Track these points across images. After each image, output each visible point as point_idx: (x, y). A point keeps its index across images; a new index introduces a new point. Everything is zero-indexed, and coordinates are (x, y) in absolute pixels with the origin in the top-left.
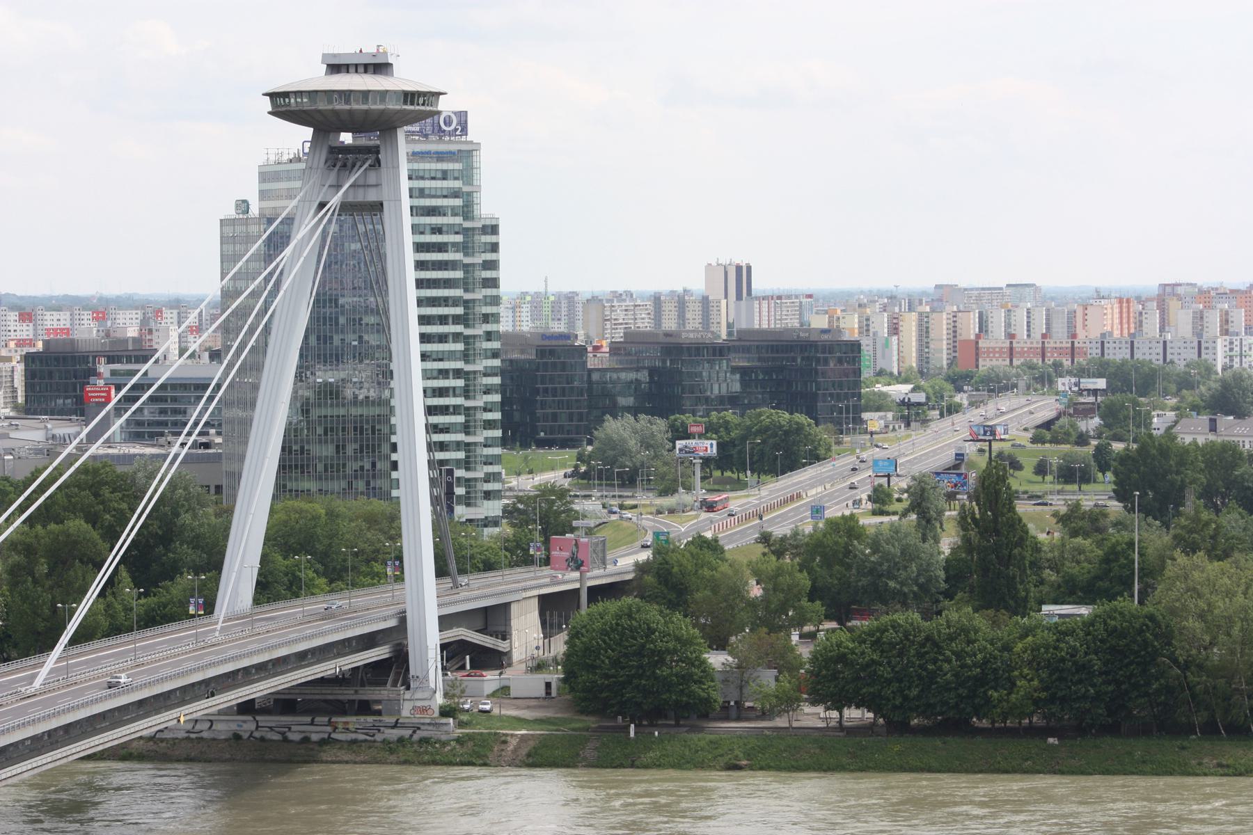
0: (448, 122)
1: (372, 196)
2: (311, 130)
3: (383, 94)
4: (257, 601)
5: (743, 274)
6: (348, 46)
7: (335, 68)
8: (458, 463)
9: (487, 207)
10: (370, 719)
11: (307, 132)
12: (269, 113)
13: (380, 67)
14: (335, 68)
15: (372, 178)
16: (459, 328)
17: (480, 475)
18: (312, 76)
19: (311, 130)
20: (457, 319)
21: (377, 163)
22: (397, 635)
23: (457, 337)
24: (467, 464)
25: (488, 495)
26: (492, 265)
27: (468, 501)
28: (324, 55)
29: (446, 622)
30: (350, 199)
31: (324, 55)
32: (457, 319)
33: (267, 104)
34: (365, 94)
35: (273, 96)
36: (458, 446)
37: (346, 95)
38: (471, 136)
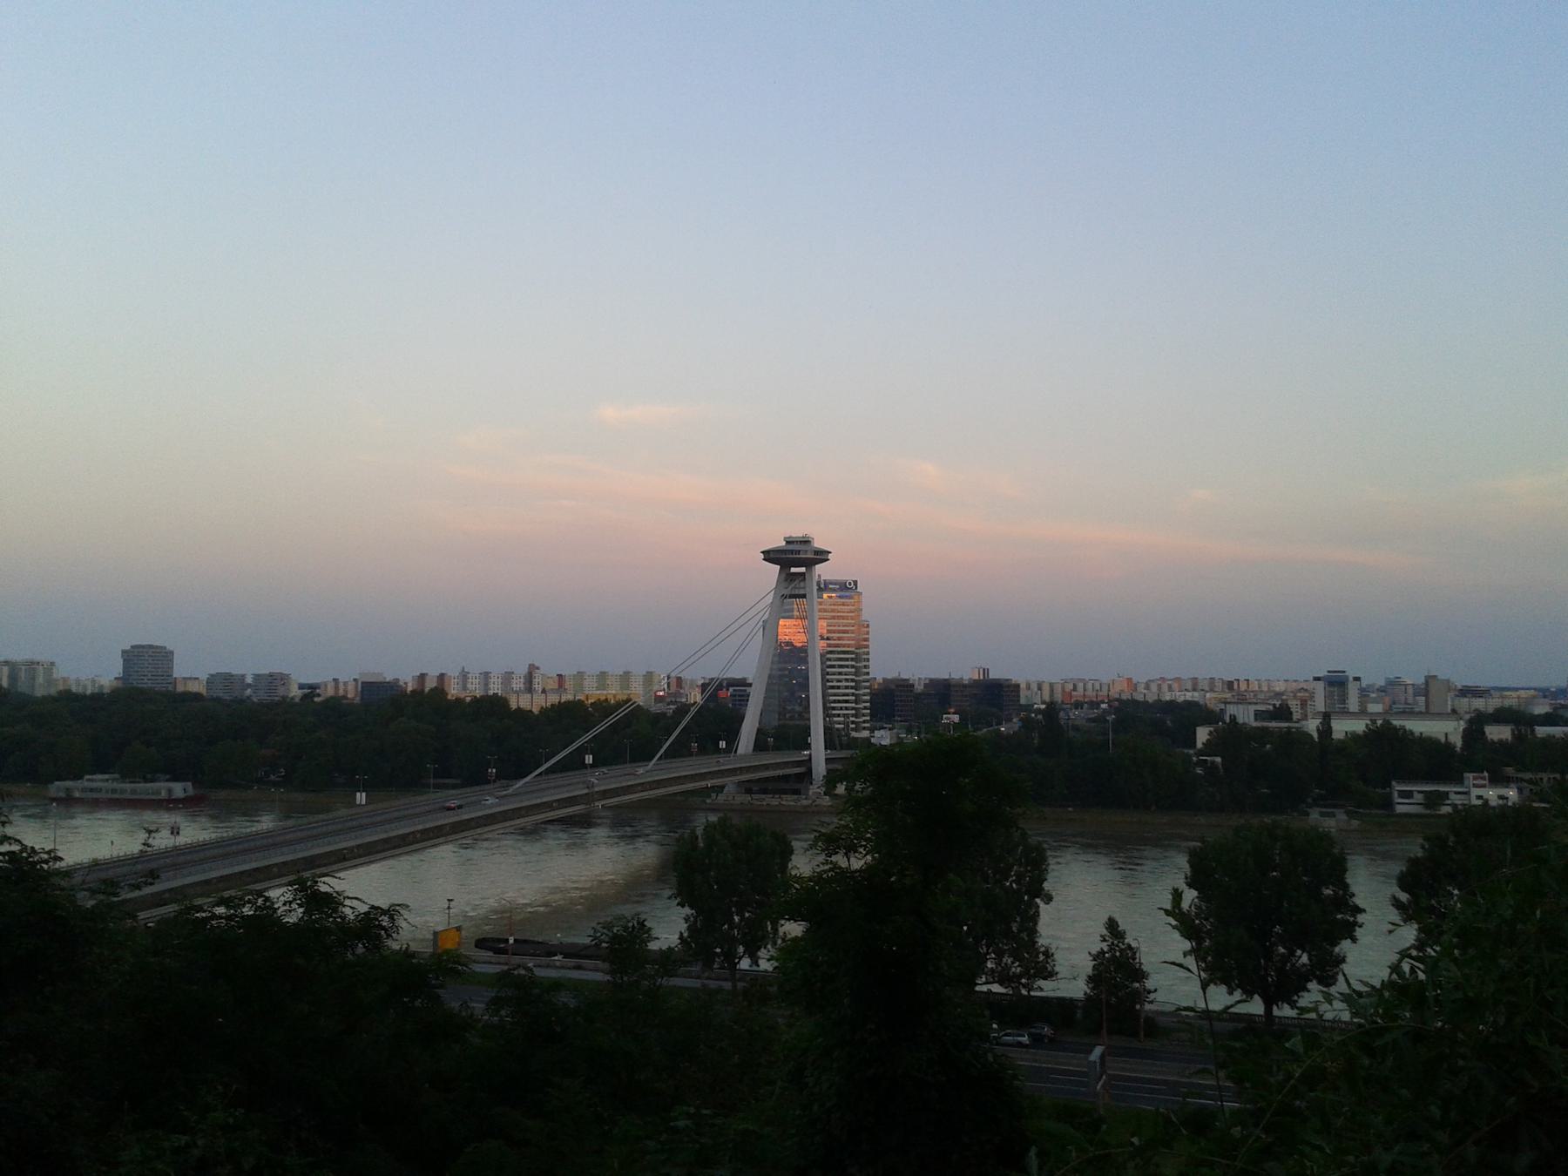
0: (850, 584)
1: (802, 592)
2: (779, 567)
4: (754, 750)
5: (986, 671)
6: (797, 533)
8: (853, 715)
9: (865, 616)
10: (796, 797)
12: (764, 559)
16: (853, 663)
17: (861, 720)
19: (779, 567)
20: (852, 659)
21: (805, 579)
23: (853, 666)
24: (856, 716)
26: (866, 640)
27: (856, 730)
28: (785, 538)
30: (793, 593)
31: (785, 538)
32: (852, 659)
33: (762, 556)
36: (853, 708)
37: (792, 552)
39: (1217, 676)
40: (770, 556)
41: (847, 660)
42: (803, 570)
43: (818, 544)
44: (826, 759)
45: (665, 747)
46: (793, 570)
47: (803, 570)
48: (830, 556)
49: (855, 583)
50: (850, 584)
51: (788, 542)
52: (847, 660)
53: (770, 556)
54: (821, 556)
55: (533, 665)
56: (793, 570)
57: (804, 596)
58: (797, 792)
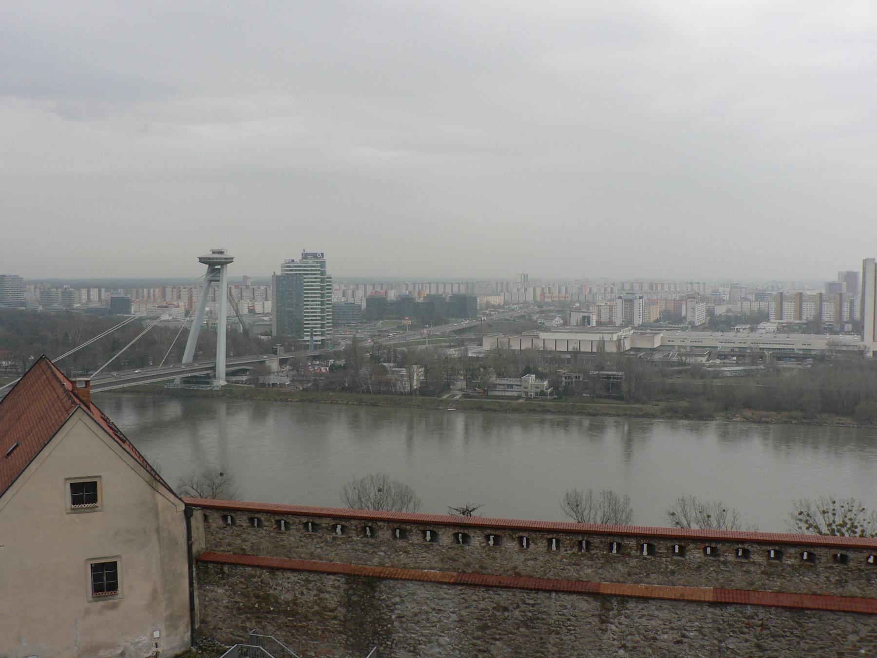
0: (319, 255)
1: (218, 279)
3: (221, 258)
6: (218, 248)
11: (208, 265)
13: (221, 253)
14: (214, 253)
15: (218, 275)
18: (207, 254)
21: (219, 272)
22: (213, 368)
25: (328, 334)
29: (227, 366)
31: (211, 250)
32: (319, 297)
34: (217, 258)
35: (200, 259)
37: (213, 258)
38: (324, 258)
40: (202, 260)
41: (316, 297)
43: (228, 254)
44: (226, 365)
46: (217, 267)
48: (234, 260)
49: (322, 254)
50: (319, 255)
51: (214, 253)
52: (316, 297)
53: (202, 260)
54: (229, 260)
55: (246, 276)
56: (217, 267)
57: (219, 281)
58: (208, 383)
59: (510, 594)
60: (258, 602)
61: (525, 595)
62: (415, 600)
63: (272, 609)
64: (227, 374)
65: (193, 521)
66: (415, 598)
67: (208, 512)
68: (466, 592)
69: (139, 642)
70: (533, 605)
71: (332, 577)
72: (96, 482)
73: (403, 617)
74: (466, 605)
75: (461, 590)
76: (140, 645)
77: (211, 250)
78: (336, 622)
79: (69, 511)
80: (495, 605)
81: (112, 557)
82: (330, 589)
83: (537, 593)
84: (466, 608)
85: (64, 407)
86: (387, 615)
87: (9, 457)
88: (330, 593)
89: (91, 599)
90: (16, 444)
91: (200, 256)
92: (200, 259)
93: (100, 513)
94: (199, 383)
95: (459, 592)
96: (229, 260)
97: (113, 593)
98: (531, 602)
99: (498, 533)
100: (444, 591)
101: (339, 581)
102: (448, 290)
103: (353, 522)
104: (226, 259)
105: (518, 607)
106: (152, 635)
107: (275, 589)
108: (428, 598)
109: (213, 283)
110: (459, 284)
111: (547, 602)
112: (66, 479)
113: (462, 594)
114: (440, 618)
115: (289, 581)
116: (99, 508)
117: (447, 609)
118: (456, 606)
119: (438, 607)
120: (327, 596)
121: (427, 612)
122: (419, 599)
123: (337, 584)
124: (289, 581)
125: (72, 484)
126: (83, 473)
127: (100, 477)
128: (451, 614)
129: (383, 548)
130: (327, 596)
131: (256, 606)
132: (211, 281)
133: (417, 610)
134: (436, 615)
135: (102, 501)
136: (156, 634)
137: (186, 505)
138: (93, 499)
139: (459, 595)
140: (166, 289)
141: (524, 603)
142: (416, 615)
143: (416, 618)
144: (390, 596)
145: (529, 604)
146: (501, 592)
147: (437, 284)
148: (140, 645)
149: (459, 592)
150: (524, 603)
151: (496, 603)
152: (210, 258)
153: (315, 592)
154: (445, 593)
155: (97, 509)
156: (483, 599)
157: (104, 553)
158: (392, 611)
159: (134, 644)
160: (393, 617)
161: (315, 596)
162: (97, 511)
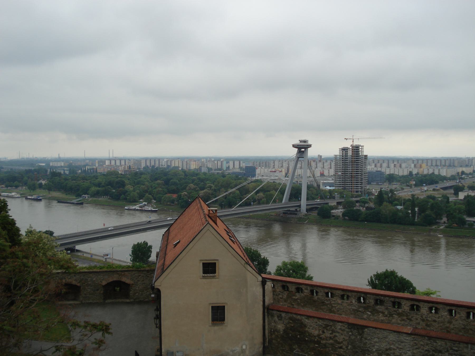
1: (303, 157)
2: (297, 149)
6: (303, 139)
7: (301, 141)
11: (297, 149)
13: (305, 142)
21: (304, 153)
22: (299, 206)
31: (299, 141)
34: (302, 145)
35: (293, 145)
37: (300, 145)
39: (306, 202)
40: (294, 146)
42: (303, 150)
43: (309, 143)
44: (307, 205)
45: (238, 204)
47: (303, 150)
48: (312, 146)
53: (294, 146)
57: (303, 157)
58: (296, 214)
59: (443, 343)
60: (299, 335)
61: (452, 344)
62: (387, 341)
63: (307, 339)
64: (307, 210)
65: (266, 287)
66: (387, 340)
67: (275, 282)
68: (417, 339)
69: (235, 350)
70: (457, 351)
71: (340, 324)
72: (215, 263)
73: (380, 351)
74: (417, 347)
75: (414, 338)
76: (236, 352)
77: (299, 141)
78: (342, 350)
79: (201, 277)
80: (434, 349)
81: (223, 303)
82: (340, 331)
83: (459, 344)
84: (417, 348)
85: (202, 223)
86: (370, 348)
87: (175, 248)
88: (339, 333)
89: (211, 325)
90: (179, 241)
91: (293, 144)
92: (293, 145)
93: (217, 280)
94: (291, 214)
95: (412, 339)
96: (310, 146)
97: (222, 323)
98: (456, 349)
99: (436, 306)
100: (403, 338)
101: (344, 326)
102: (148, 164)
103: (353, 294)
104: (308, 145)
105: (448, 351)
106: (242, 347)
107: (309, 328)
108: (394, 341)
109: (300, 159)
110: (217, 161)
111: (465, 350)
112: (201, 260)
113: (415, 340)
114: (401, 353)
115: (317, 324)
116: (217, 277)
117: (405, 348)
118: (410, 347)
119: (400, 347)
120: (337, 334)
121: (394, 349)
122: (389, 341)
123: (343, 328)
124: (317, 324)
125: (203, 263)
126: (209, 257)
127: (218, 260)
128: (408, 352)
129: (370, 310)
130: (337, 334)
131: (298, 336)
132: (299, 158)
133: (388, 347)
134: (399, 351)
135: (219, 273)
136: (244, 347)
137: (263, 278)
138: (214, 272)
139: (412, 341)
140: (275, 162)
141: (452, 349)
142: (387, 350)
143: (387, 352)
144: (372, 338)
145: (454, 350)
146: (437, 341)
147: (388, 161)
148: (236, 352)
149: (412, 339)
150: (452, 349)
151: (434, 348)
152: (298, 145)
153: (330, 332)
154: (405, 339)
155: (216, 277)
156: (427, 344)
157: (218, 301)
158: (374, 346)
159: (233, 351)
160: (374, 350)
161: (331, 334)
162: (216, 278)
